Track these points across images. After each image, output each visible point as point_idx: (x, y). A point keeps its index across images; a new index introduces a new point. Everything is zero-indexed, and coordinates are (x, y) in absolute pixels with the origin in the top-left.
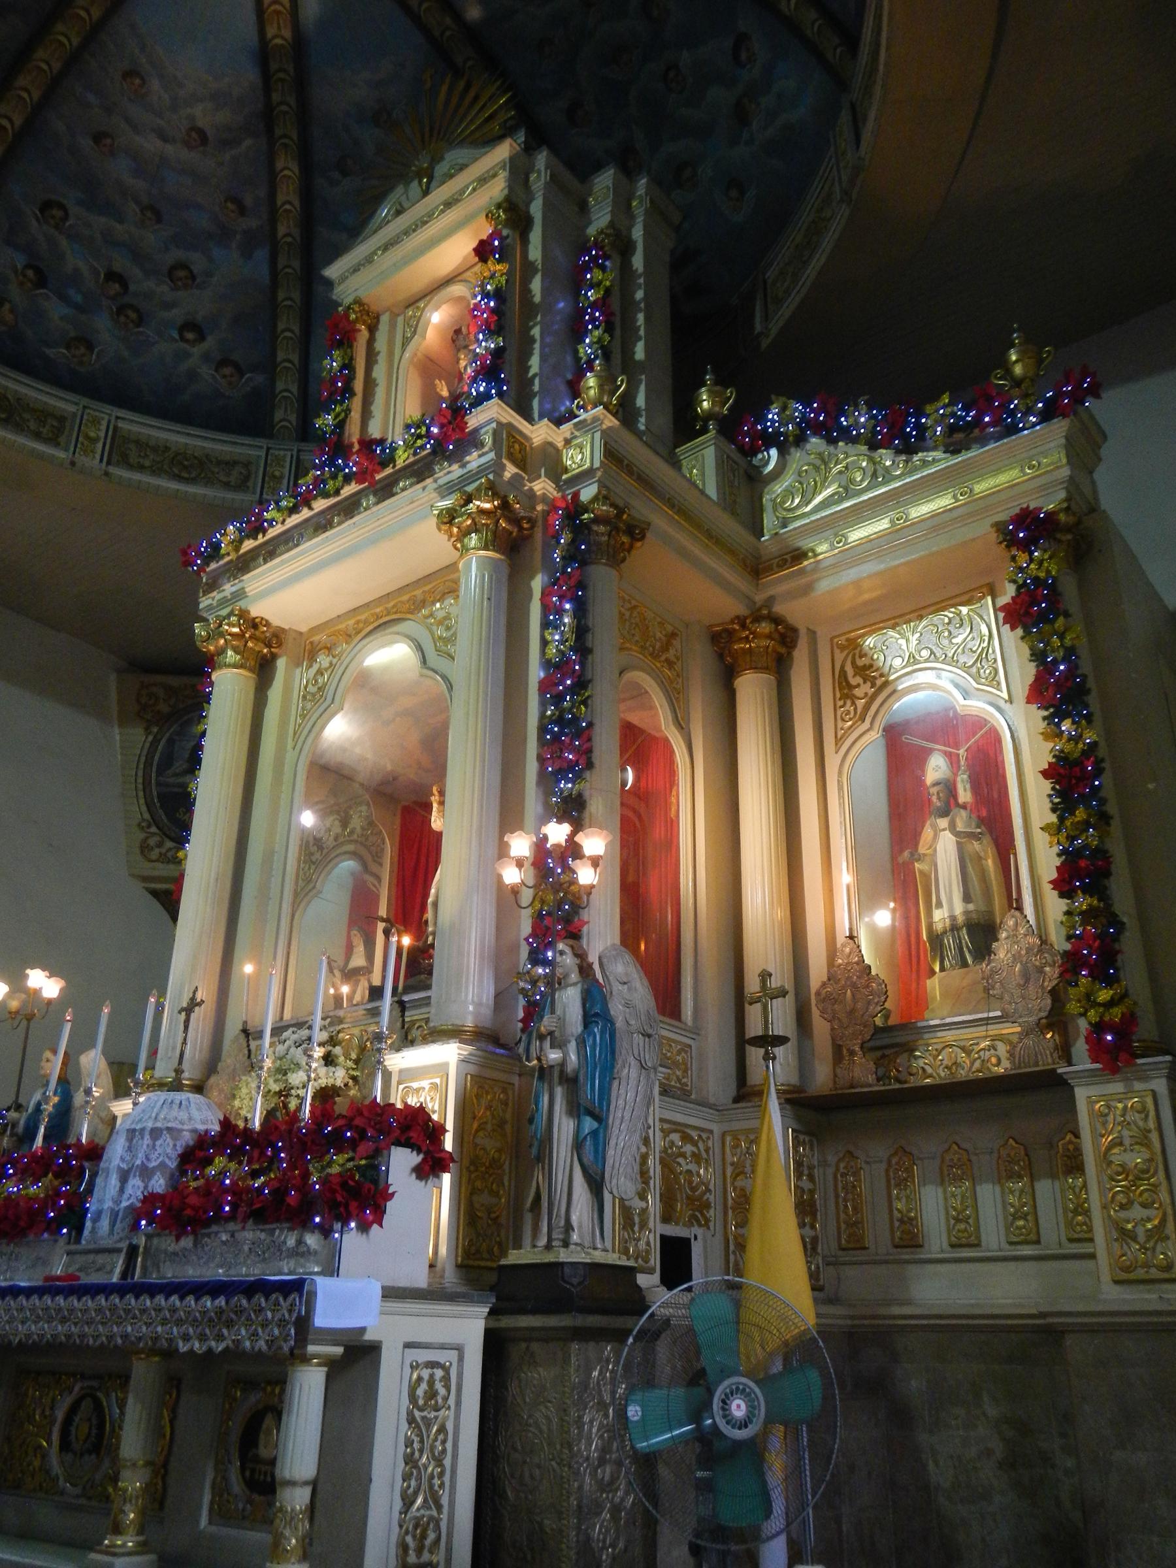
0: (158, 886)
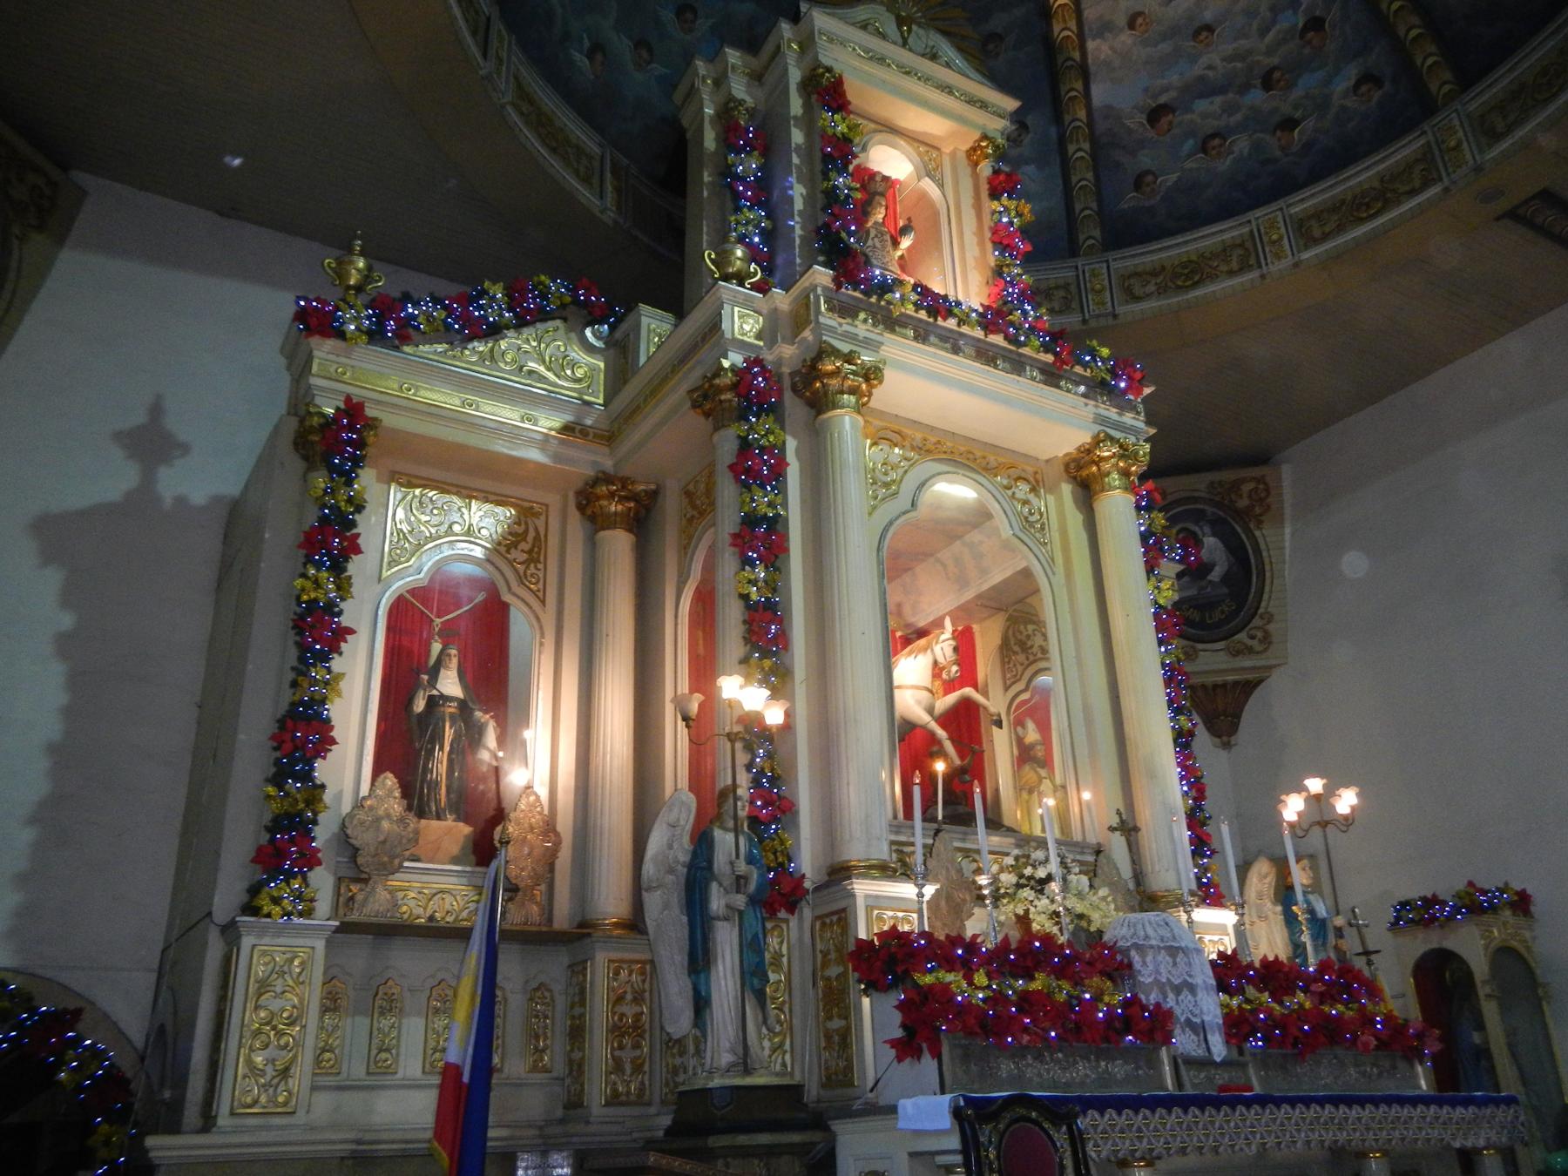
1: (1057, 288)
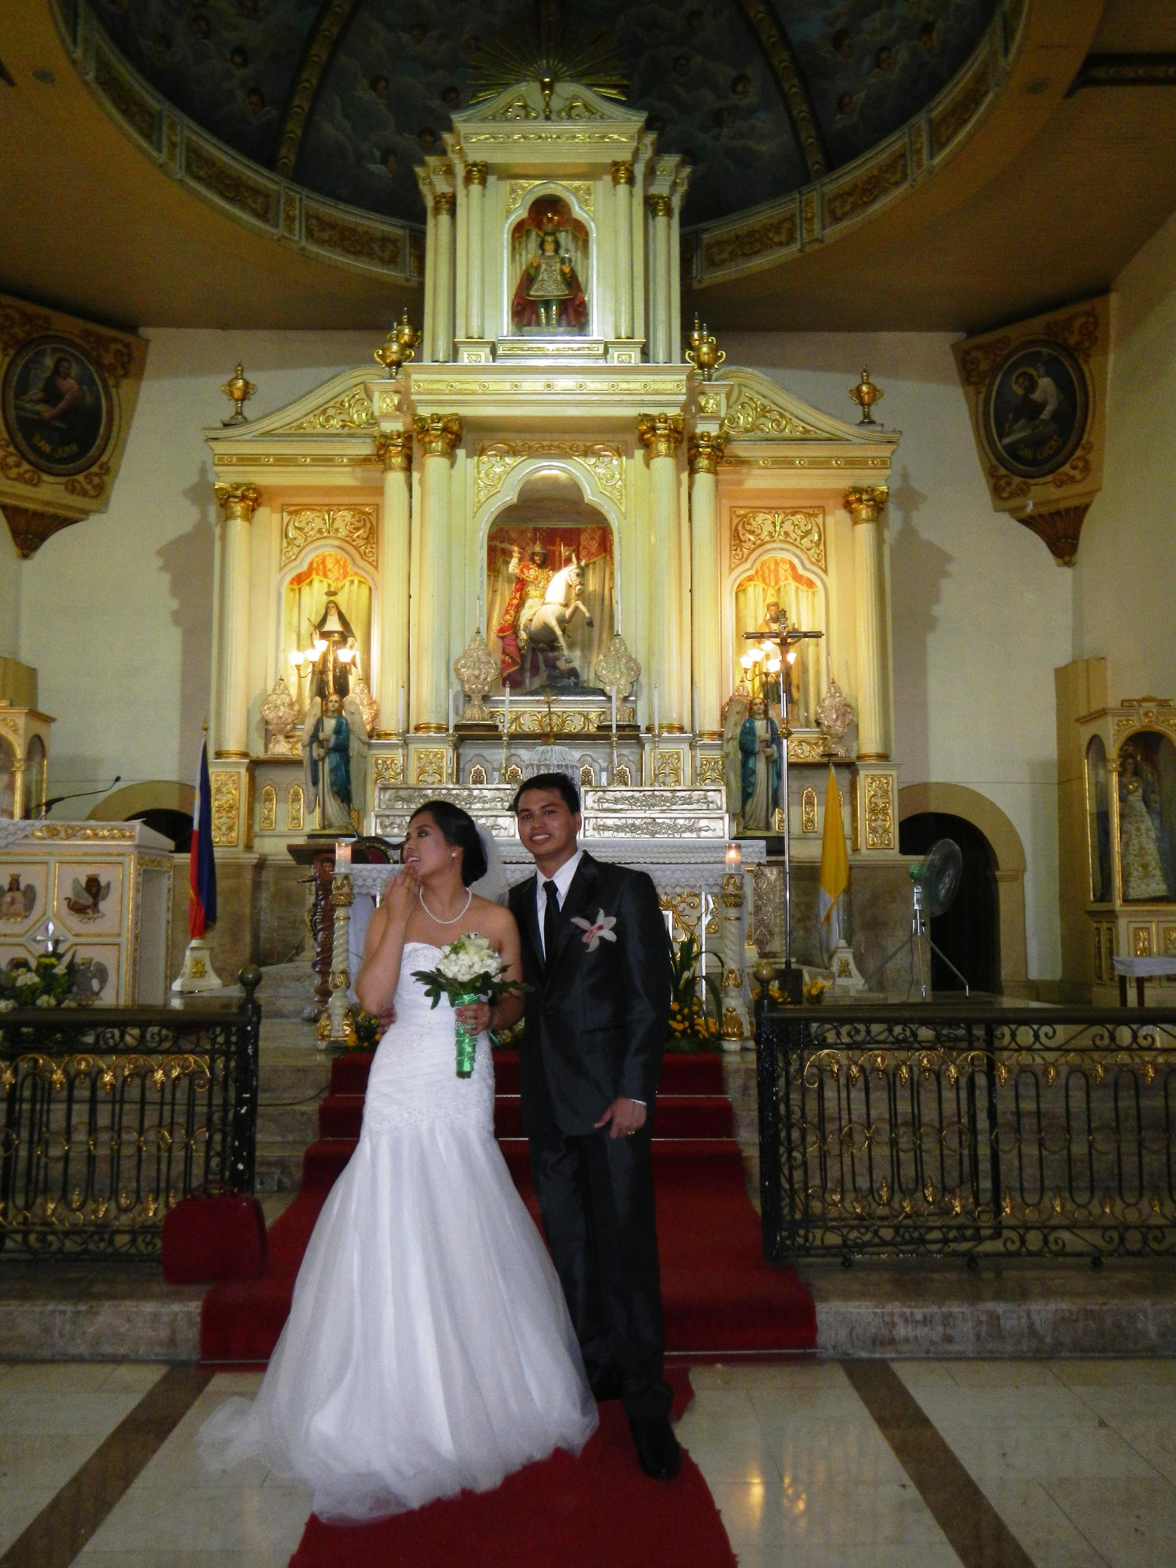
1: (786, 220)
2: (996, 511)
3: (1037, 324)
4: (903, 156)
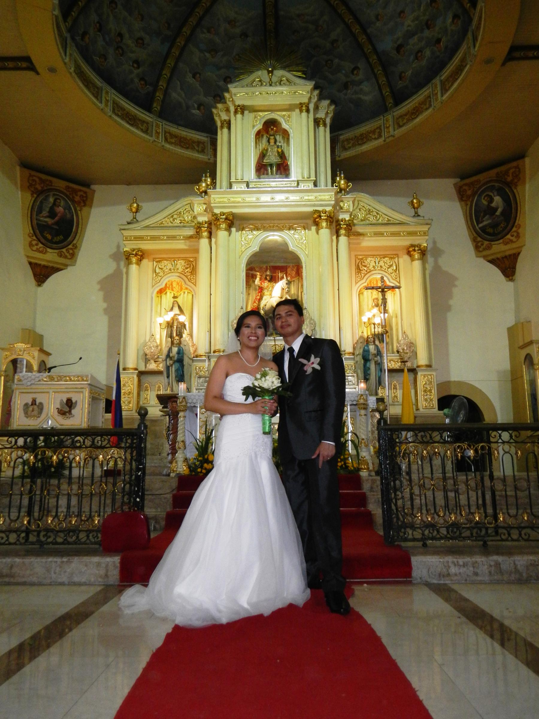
0: (33, 261)
1: (377, 128)
2: (477, 257)
3: (493, 173)
4: (429, 97)
